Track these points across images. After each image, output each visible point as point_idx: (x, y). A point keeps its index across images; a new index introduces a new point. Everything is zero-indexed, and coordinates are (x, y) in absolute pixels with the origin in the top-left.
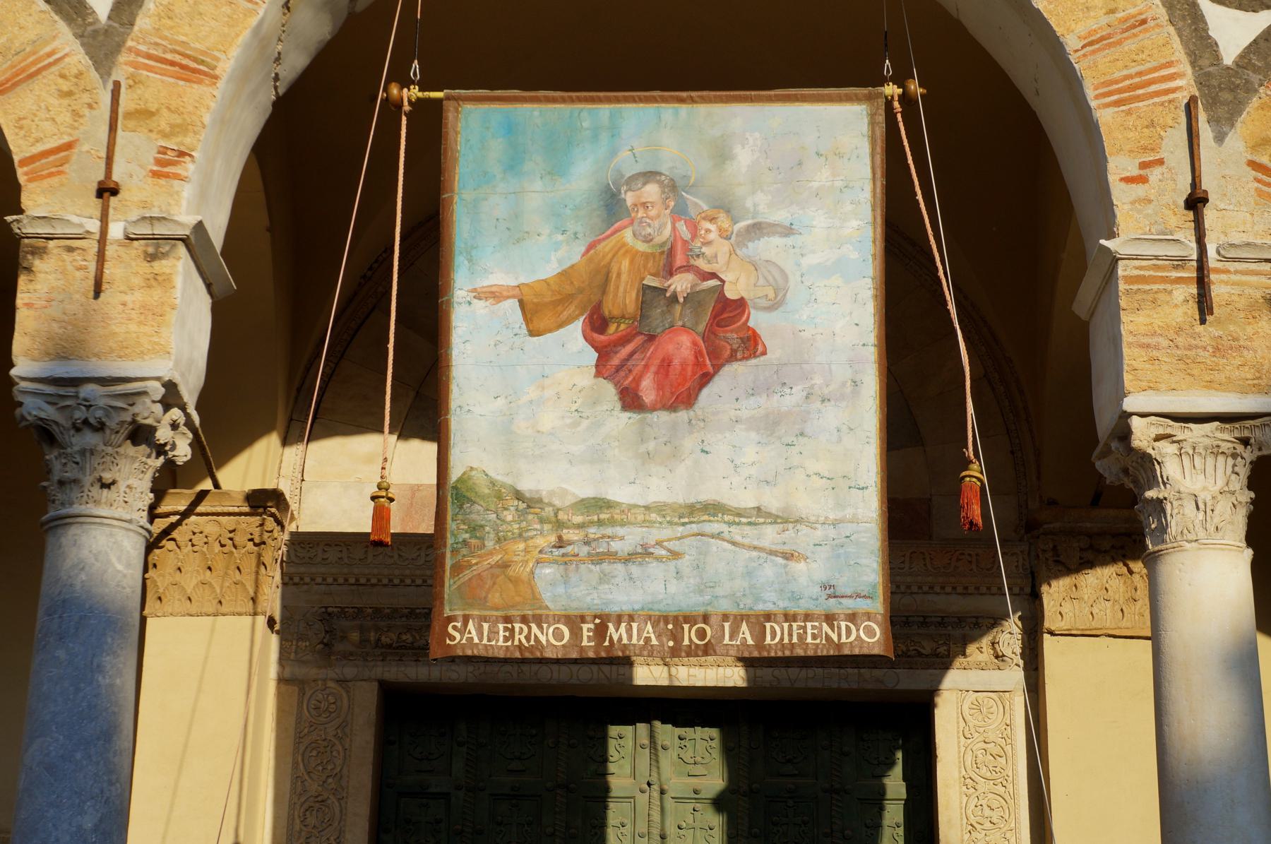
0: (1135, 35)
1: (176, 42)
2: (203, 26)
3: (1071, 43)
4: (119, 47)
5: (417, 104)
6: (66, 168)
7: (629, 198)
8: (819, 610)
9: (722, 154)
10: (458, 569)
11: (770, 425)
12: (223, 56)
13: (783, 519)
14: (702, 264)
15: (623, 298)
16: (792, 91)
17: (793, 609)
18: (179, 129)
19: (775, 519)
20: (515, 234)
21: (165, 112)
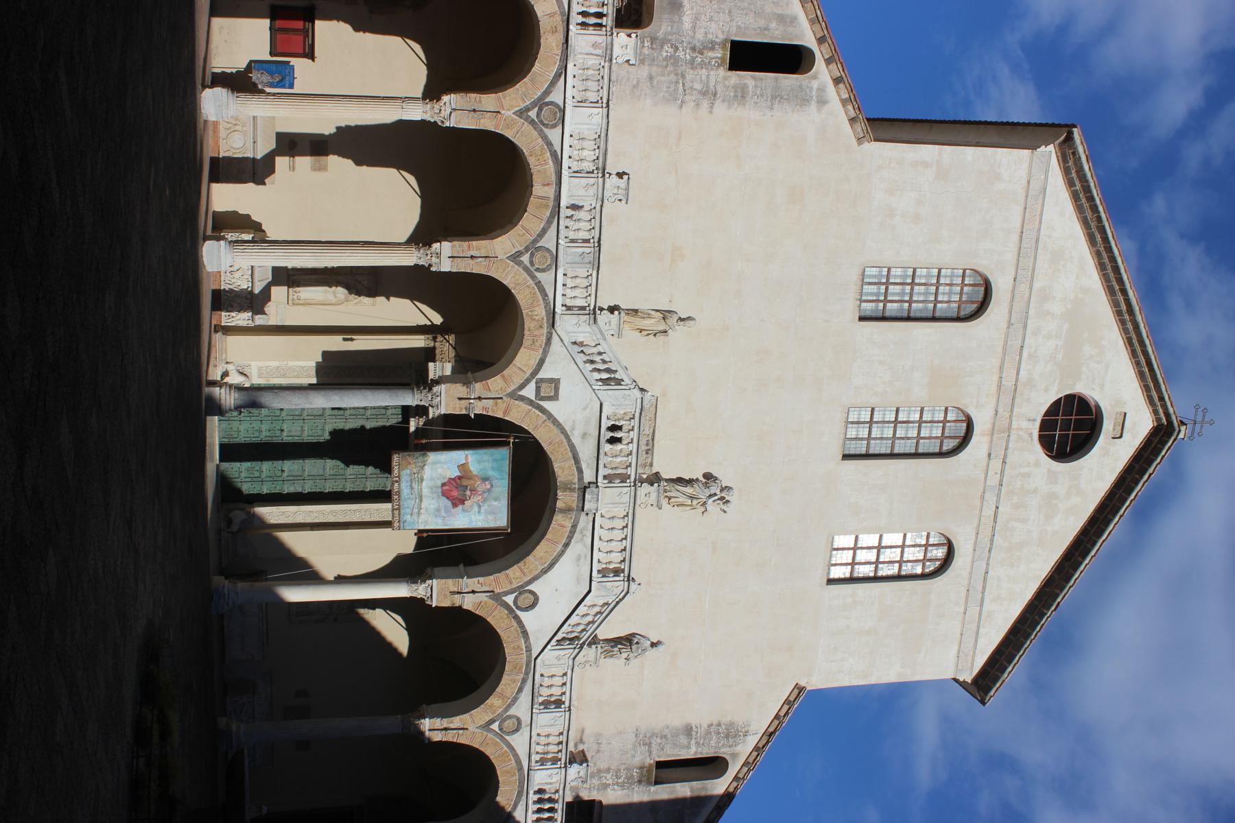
3: (507, 571)
5: (509, 442)
8: (401, 519)
9: (496, 499)
10: (409, 455)
11: (438, 510)
13: (419, 514)
14: (472, 496)
15: (465, 482)
17: (401, 516)
19: (419, 511)
20: (479, 462)
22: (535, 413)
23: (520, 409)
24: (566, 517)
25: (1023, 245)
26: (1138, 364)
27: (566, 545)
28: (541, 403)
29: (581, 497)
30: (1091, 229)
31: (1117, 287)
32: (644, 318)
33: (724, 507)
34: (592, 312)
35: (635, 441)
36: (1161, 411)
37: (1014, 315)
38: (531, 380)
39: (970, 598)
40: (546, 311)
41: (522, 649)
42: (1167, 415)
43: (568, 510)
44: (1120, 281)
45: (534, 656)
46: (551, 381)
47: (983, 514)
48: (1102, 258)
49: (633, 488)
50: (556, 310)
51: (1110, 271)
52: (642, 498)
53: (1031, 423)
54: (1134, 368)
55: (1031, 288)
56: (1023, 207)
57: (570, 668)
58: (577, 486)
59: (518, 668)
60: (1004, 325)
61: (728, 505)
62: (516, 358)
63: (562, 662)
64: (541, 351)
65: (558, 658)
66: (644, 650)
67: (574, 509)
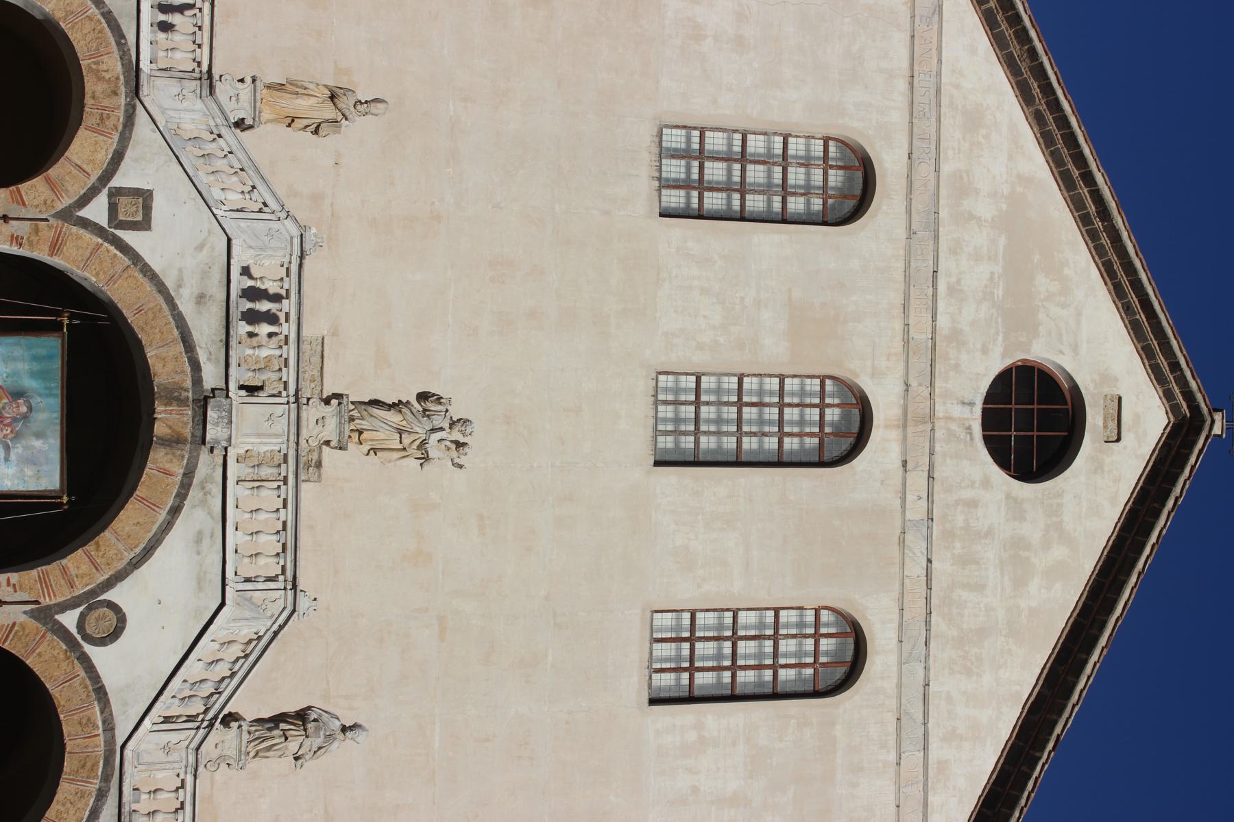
0: (67, 584)
1: (66, 240)
3: (64, 562)
4: (65, 220)
5: (61, 323)
6: (15, 204)
7: (21, 401)
9: (39, 435)
12: (61, 257)
16: (65, 462)
18: (31, 243)
21: (38, 238)
22: (108, 251)
23: (80, 243)
24: (173, 454)
25: (917, 99)
26: (1128, 308)
27: (175, 511)
28: (119, 233)
29: (199, 418)
30: (1023, 74)
31: (1076, 173)
32: (297, 94)
34: (206, 76)
36: (1177, 390)
37: (915, 217)
38: (100, 191)
39: (903, 735)
40: (123, 65)
41: (95, 726)
42: (1188, 395)
43: (174, 441)
44: (1080, 160)
45: (119, 742)
46: (137, 192)
47: (906, 573)
48: (1046, 124)
49: (293, 406)
50: (142, 66)
51: (1060, 145)
52: (310, 427)
53: (967, 408)
54: (1122, 319)
55: (937, 171)
56: (908, 34)
57: (190, 769)
58: (190, 395)
59: (89, 765)
60: (901, 233)
61: (466, 449)
62: (72, 147)
63: (174, 756)
64: (116, 137)
65: (167, 749)
66: (330, 737)
67: (186, 440)
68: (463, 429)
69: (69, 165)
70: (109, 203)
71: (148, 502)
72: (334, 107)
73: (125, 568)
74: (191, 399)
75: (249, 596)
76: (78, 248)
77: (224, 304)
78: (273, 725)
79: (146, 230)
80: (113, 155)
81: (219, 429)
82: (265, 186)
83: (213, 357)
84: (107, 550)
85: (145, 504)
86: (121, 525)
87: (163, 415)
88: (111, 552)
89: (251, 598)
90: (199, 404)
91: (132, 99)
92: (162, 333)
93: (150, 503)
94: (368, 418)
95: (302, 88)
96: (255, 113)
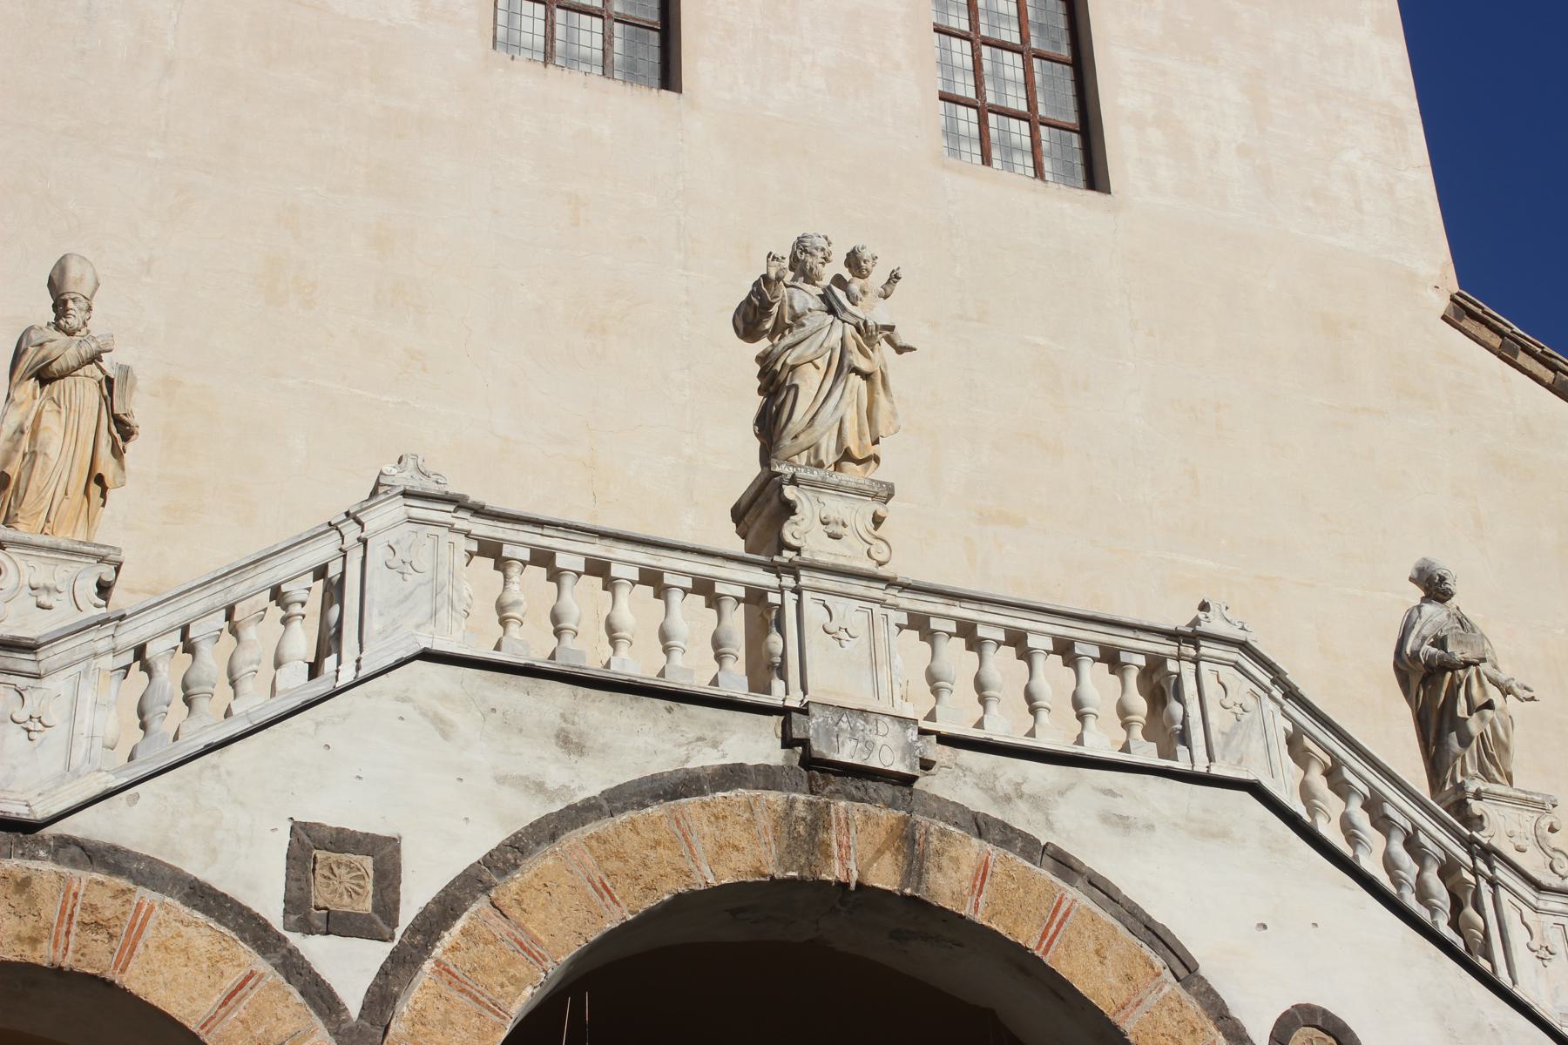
2: (454, 1035)
22: (454, 949)
23: (434, 1016)
27: (1064, 865)
28: (408, 913)
29: (851, 785)
33: (878, 278)
35: (599, 549)
38: (293, 952)
49: (806, 579)
58: (802, 797)
61: (866, 254)
62: (174, 1010)
67: (906, 821)
68: (820, 254)
69: (225, 1025)
70: (328, 933)
71: (1049, 925)
72: (69, 380)
73: (1196, 995)
74: (812, 798)
75: (1220, 736)
76: (447, 1022)
77: (581, 691)
78: (1454, 733)
79: (398, 850)
80: (195, 907)
81: (879, 741)
82: (277, 560)
83: (709, 734)
84: (1164, 1031)
85: (1056, 933)
86: (1106, 993)
87: (852, 866)
88: (1167, 1020)
89: (1223, 733)
90: (820, 782)
91: (43, 843)
92: (658, 843)
93: (1053, 917)
94: (817, 434)
95: (19, 441)
96: (87, 555)
